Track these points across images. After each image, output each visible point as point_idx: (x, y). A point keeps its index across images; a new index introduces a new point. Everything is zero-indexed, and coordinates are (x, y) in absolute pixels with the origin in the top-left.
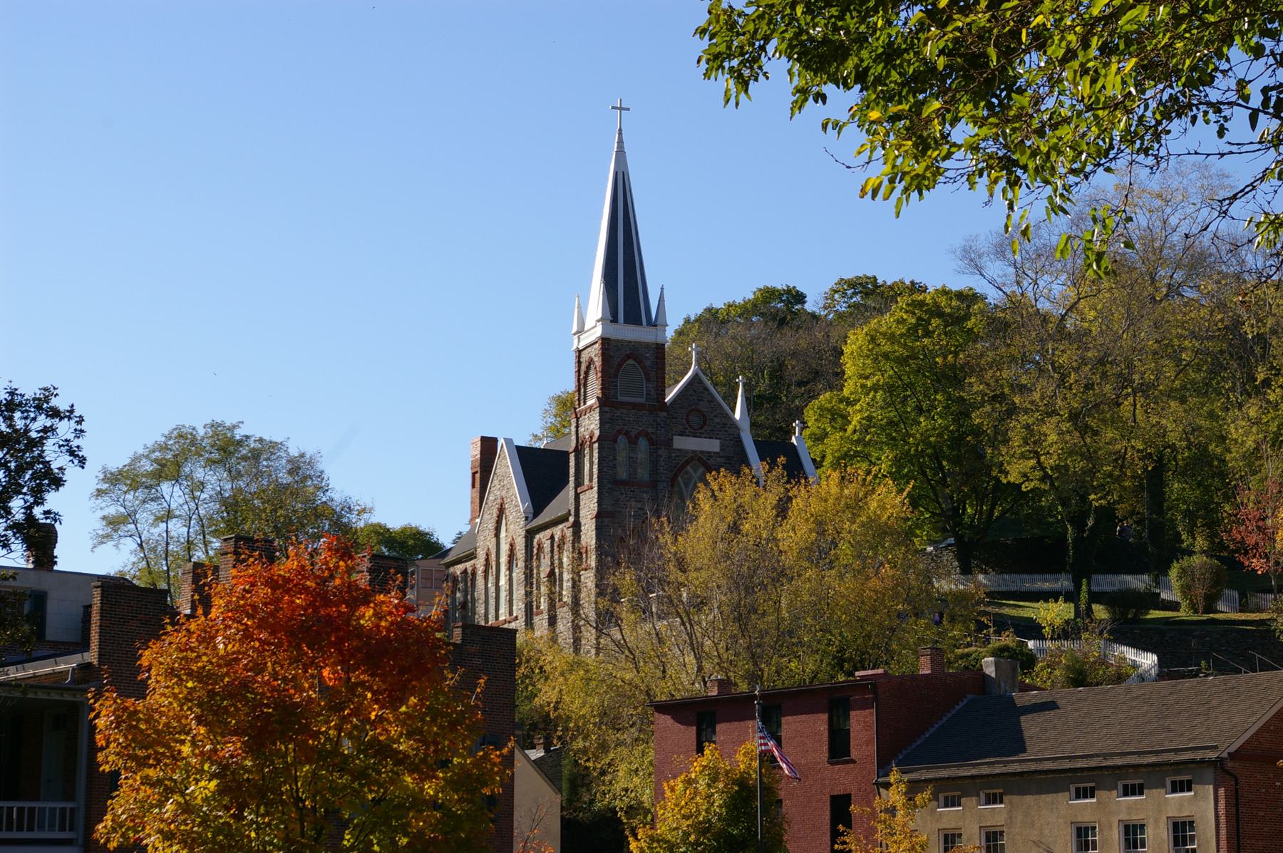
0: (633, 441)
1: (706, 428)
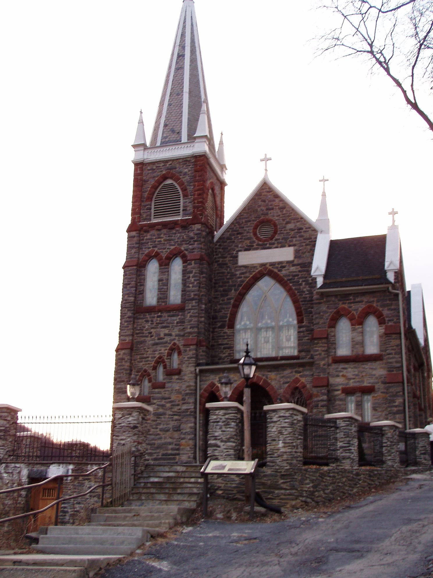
1: (276, 237)
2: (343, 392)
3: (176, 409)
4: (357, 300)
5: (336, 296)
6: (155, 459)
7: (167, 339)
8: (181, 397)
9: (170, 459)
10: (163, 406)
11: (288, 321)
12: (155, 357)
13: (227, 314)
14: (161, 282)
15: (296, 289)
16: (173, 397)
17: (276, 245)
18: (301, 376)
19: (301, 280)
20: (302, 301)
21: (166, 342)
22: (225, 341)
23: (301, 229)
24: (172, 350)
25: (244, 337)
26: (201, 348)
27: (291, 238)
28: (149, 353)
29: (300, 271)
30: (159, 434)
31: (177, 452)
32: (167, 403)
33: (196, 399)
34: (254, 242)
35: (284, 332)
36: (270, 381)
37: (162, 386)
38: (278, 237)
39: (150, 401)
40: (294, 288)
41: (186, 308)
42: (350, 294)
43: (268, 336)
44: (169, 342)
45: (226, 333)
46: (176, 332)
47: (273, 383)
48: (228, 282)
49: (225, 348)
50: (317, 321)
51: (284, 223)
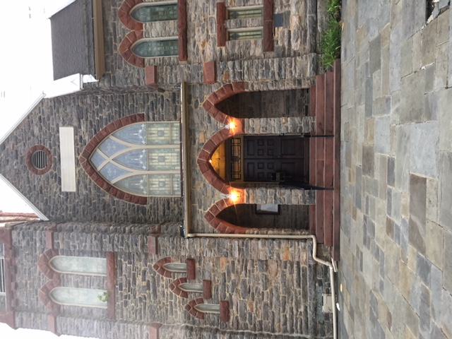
0: (58, 278)
2: (224, 45)
3: (238, 267)
4: (112, 31)
5: (106, 58)
6: (305, 296)
7: (149, 277)
8: (223, 259)
9: (304, 276)
10: (234, 285)
11: (142, 134)
12: (171, 294)
13: (129, 205)
14: (80, 285)
15: (106, 124)
16: (223, 269)
17: (57, 147)
18: (202, 100)
19: (96, 118)
20: (120, 117)
21: (153, 277)
22: (161, 208)
23: (40, 118)
24: (163, 271)
25: (158, 186)
26: (162, 231)
27: (49, 130)
28: (165, 302)
29: (87, 120)
30: (271, 291)
31: (295, 266)
32: (230, 278)
33: (226, 238)
34: (51, 173)
35: (153, 138)
36: (207, 141)
37: (209, 284)
38: (48, 144)
39: (228, 302)
40: (104, 126)
41: (111, 250)
42: (105, 39)
43: (157, 158)
44: (152, 275)
45: (151, 207)
46: (141, 265)
47: (209, 136)
48: (95, 203)
49: (169, 209)
50: (135, 81)
51: (32, 138)
